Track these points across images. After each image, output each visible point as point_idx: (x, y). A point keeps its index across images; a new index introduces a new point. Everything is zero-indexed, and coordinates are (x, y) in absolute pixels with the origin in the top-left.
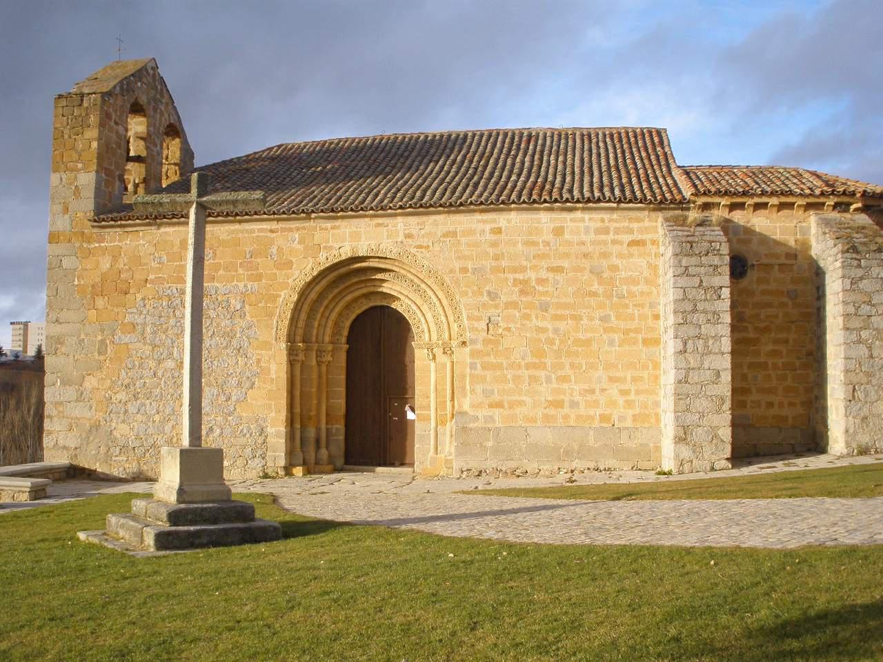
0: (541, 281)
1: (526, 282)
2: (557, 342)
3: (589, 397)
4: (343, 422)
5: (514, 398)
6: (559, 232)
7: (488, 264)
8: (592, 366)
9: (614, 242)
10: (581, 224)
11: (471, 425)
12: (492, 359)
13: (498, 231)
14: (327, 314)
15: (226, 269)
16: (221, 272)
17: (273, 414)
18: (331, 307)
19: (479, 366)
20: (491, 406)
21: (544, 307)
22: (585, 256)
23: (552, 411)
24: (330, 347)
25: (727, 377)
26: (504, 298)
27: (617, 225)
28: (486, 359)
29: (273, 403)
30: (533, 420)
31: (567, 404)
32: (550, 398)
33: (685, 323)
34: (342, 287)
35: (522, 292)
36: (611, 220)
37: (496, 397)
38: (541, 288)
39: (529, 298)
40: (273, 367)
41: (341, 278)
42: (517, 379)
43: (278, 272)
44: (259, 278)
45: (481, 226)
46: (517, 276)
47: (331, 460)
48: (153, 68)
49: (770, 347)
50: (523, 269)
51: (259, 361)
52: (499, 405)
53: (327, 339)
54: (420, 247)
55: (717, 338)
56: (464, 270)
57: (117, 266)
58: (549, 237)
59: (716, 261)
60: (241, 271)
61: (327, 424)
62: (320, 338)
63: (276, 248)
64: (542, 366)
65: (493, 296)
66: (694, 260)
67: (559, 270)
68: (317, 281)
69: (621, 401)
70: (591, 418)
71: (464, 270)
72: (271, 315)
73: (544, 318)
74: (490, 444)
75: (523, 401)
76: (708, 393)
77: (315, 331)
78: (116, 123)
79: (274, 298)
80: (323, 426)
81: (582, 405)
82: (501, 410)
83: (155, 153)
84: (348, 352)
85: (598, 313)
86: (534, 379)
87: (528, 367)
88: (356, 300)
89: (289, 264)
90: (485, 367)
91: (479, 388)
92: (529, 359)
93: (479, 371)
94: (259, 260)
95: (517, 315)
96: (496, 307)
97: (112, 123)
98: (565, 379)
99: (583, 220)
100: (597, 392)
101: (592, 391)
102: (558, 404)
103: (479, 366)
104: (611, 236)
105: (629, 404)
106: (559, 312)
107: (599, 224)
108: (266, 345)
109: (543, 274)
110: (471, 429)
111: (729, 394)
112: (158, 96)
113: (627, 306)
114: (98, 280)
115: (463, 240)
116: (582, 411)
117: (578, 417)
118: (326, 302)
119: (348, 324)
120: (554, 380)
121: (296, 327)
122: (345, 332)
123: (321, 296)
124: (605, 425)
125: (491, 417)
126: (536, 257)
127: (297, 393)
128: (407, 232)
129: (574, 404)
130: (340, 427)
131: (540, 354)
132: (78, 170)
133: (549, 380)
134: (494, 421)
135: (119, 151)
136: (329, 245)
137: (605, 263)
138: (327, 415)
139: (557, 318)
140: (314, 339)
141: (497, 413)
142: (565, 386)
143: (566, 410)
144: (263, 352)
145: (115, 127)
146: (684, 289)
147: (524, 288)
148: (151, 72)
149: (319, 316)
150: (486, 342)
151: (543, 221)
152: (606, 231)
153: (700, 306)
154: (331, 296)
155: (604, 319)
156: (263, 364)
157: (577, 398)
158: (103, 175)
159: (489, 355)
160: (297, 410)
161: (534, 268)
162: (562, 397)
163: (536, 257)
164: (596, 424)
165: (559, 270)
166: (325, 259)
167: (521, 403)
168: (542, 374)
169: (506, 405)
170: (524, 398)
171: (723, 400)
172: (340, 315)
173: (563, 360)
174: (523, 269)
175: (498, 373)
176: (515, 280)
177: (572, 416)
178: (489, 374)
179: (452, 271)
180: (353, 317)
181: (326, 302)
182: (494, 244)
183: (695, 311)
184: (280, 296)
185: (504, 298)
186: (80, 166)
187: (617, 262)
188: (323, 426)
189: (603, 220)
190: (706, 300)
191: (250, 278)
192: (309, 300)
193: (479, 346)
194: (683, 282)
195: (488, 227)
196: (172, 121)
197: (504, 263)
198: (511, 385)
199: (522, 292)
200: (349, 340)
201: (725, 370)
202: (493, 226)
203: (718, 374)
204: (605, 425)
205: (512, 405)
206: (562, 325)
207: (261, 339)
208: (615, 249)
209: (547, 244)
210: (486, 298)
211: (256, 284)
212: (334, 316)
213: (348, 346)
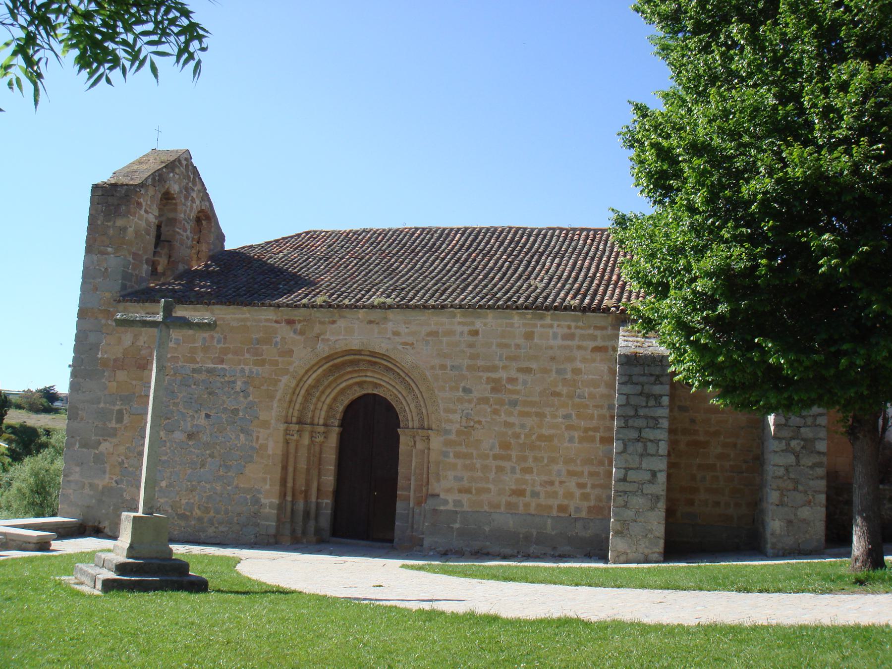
0: (511, 380)
1: (497, 381)
2: (523, 436)
3: (549, 488)
4: (331, 496)
5: (479, 485)
6: (529, 336)
7: (466, 362)
8: (552, 460)
9: (579, 347)
10: (551, 331)
11: (442, 508)
12: (463, 449)
13: (475, 333)
14: (323, 399)
15: (236, 353)
16: (230, 356)
17: (268, 487)
18: (327, 393)
19: (451, 455)
20: (460, 491)
21: (514, 403)
22: (553, 359)
23: (514, 499)
24: (321, 429)
25: (662, 478)
26: (476, 394)
27: (583, 332)
29: (268, 477)
30: (498, 506)
31: (528, 493)
32: (513, 487)
33: (627, 427)
34: (336, 375)
35: (494, 390)
36: (577, 327)
37: (465, 483)
38: (509, 387)
39: (499, 396)
40: (271, 445)
41: (337, 367)
42: (485, 468)
43: (280, 359)
44: (262, 363)
45: (459, 329)
46: (489, 374)
47: (318, 531)
48: (186, 159)
49: (719, 450)
50: (494, 368)
51: (258, 438)
52: (468, 491)
53: (321, 422)
54: (406, 344)
55: (656, 442)
56: (443, 367)
57: (138, 343)
58: (521, 341)
60: (247, 356)
61: (318, 498)
63: (280, 337)
64: (508, 458)
65: (466, 390)
67: (528, 370)
69: (578, 493)
70: (551, 507)
71: (443, 367)
72: (271, 397)
73: (510, 414)
74: (457, 526)
76: (645, 492)
77: (310, 414)
78: (146, 212)
79: (276, 382)
80: (313, 499)
81: (542, 495)
82: (470, 496)
83: (185, 238)
85: (562, 412)
86: (500, 469)
87: (495, 457)
88: (349, 387)
89: (290, 353)
90: (457, 455)
91: (451, 474)
92: (497, 451)
93: (451, 459)
94: (264, 347)
95: (489, 410)
96: (470, 401)
97: (142, 212)
98: (527, 470)
99: (551, 326)
100: (557, 483)
101: (551, 483)
102: (520, 493)
103: (451, 455)
104: (576, 342)
105: (585, 497)
106: (527, 409)
107: (566, 331)
108: (265, 424)
109: (513, 374)
110: (441, 511)
111: (664, 493)
112: (190, 185)
113: (586, 406)
114: (120, 355)
115: (444, 339)
116: (542, 500)
117: (539, 506)
118: (321, 388)
119: (341, 408)
120: (518, 471)
122: (339, 416)
123: (318, 381)
124: (562, 515)
125: (460, 501)
126: (509, 358)
127: (291, 469)
128: (395, 329)
129: (535, 494)
130: (327, 502)
131: (506, 446)
132: (108, 254)
133: (513, 470)
134: (462, 506)
136: (326, 337)
137: (569, 367)
138: (319, 490)
139: (523, 414)
141: (465, 498)
142: (528, 477)
143: (528, 499)
144: (262, 430)
145: (145, 215)
146: (628, 396)
147: (497, 387)
148: (184, 163)
149: (314, 400)
150: (459, 433)
151: (516, 325)
152: (571, 337)
153: (642, 412)
155: (567, 417)
156: (260, 441)
157: (538, 488)
158: (131, 259)
159: (461, 445)
160: (290, 484)
161: (505, 368)
162: (524, 487)
163: (509, 358)
164: (555, 513)
165: (528, 370)
166: (323, 349)
167: (488, 491)
168: (507, 465)
169: (474, 492)
170: (491, 486)
171: (658, 498)
172: (335, 399)
173: (527, 454)
174: (494, 368)
175: (468, 462)
176: (488, 378)
177: (533, 505)
178: (460, 462)
179: (433, 368)
180: (346, 402)
181: (321, 388)
182: (471, 346)
183: (636, 416)
184: (280, 381)
185: (476, 394)
186: (109, 249)
187: (582, 366)
188: (313, 499)
189: (569, 327)
190: (646, 406)
191: (257, 363)
192: (306, 386)
193: (453, 437)
194: (628, 389)
195: (466, 329)
196: (203, 208)
197: (480, 363)
198: (479, 474)
199: (494, 390)
200: (342, 424)
201: (660, 471)
202: (472, 328)
203: (654, 474)
204: (562, 515)
205: (480, 491)
206: (530, 422)
207: (261, 418)
208: (579, 354)
209: (518, 346)
211: (260, 368)
212: (328, 401)
213: (341, 429)
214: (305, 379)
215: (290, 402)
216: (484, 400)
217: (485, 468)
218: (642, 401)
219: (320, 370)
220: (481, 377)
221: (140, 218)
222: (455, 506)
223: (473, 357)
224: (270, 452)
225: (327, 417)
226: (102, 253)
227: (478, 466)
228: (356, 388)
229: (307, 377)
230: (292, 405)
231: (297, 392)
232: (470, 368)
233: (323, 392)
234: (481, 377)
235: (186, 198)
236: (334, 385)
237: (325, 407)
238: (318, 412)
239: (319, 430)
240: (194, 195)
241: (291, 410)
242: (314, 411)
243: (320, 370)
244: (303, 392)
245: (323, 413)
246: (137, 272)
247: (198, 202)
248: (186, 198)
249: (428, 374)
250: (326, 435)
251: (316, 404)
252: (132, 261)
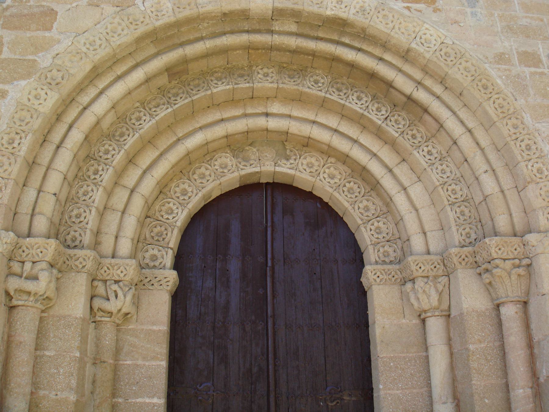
18: (145, 160)
62: (107, 244)
68: (120, 69)
77: (91, 219)
84: (178, 299)
119: (181, 217)
121: (39, 191)
140: (87, 239)
149: (107, 176)
154: (148, 125)
180: (195, 202)
192: (89, 119)
214: (85, 99)
215: (31, 164)
219: (138, 75)
225: (139, 242)
228: (227, 159)
229: (92, 92)
230: (39, 173)
231: (56, 137)
233: (131, 161)
236: (163, 143)
237: (137, 205)
238: (113, 219)
239: (117, 274)
241: (31, 194)
242: (101, 215)
243: (138, 75)
244: (76, 136)
245: (131, 224)
249: (495, 73)
250: (140, 286)
251: (109, 194)
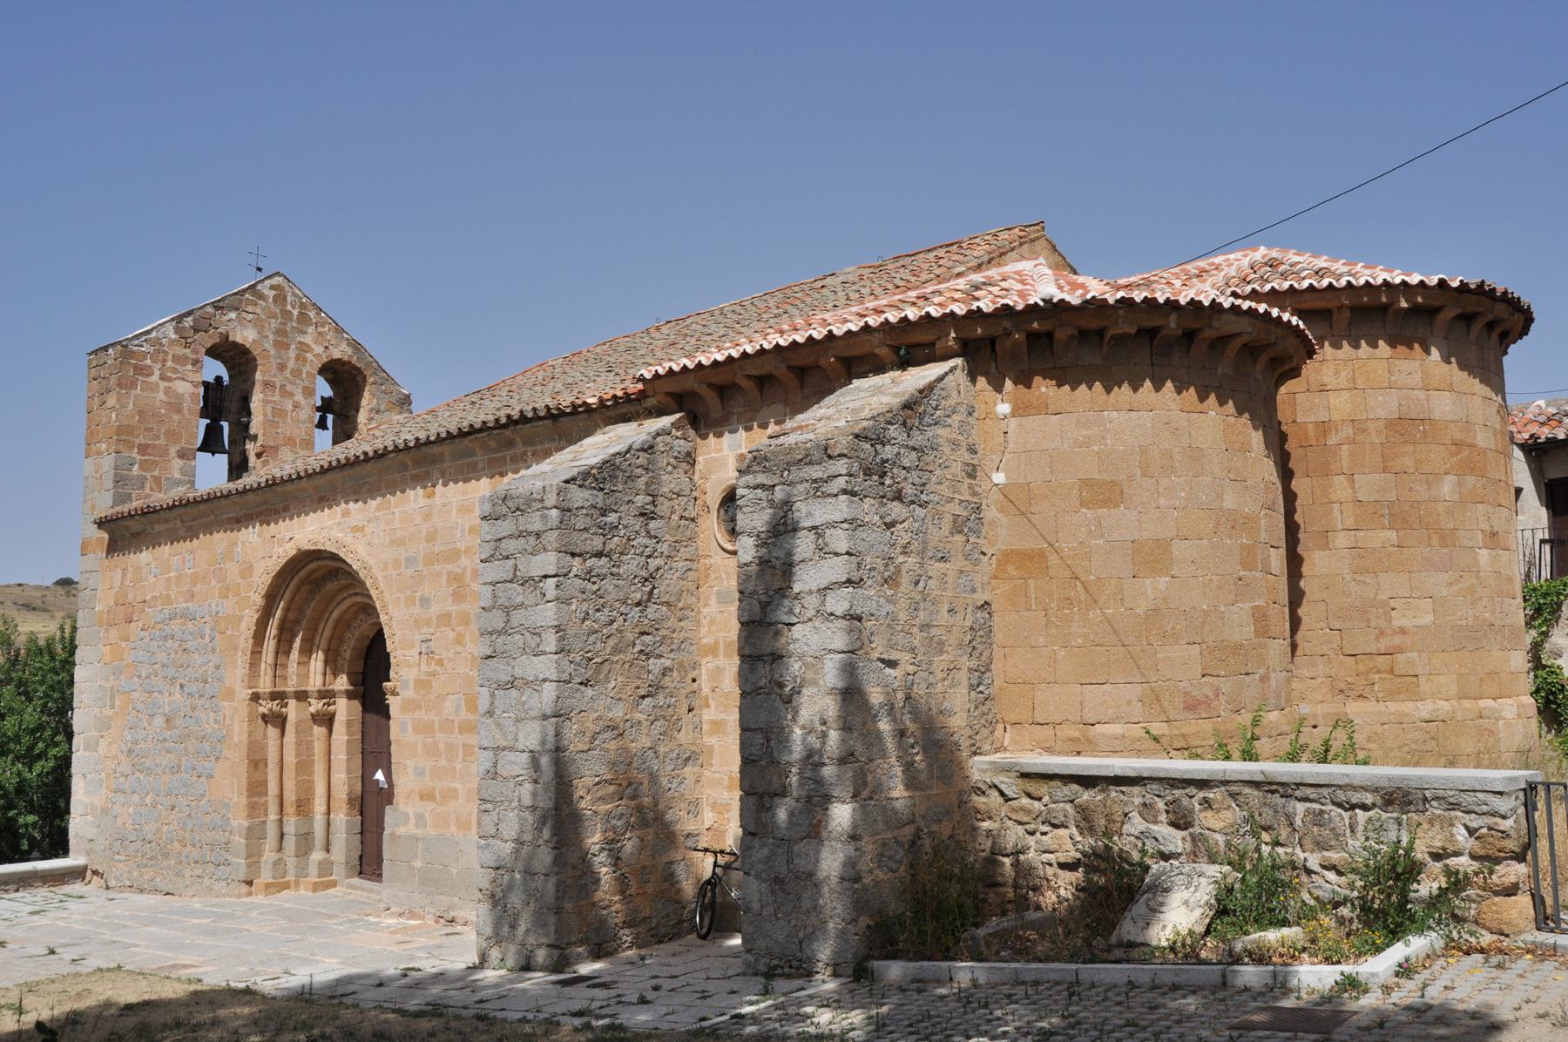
28: (420, 714)
39: (464, 606)
42: (451, 747)
47: (326, 867)
59: (534, 522)
65: (425, 602)
66: (506, 527)
74: (418, 864)
75: (456, 790)
92: (464, 714)
96: (428, 623)
135: (176, 417)
145: (163, 384)
170: (458, 786)
196: (337, 355)
197: (438, 548)
198: (444, 762)
210: (417, 610)
216: (445, 618)
217: (451, 747)
218: (517, 593)
220: (439, 575)
221: (153, 388)
222: (417, 825)
223: (431, 538)
224: (236, 740)
226: (99, 453)
227: (441, 746)
232: (430, 559)
234: (439, 575)
235: (281, 346)
240: (308, 339)
246: (156, 473)
247: (319, 349)
248: (281, 346)
249: (380, 576)
252: (138, 457)
